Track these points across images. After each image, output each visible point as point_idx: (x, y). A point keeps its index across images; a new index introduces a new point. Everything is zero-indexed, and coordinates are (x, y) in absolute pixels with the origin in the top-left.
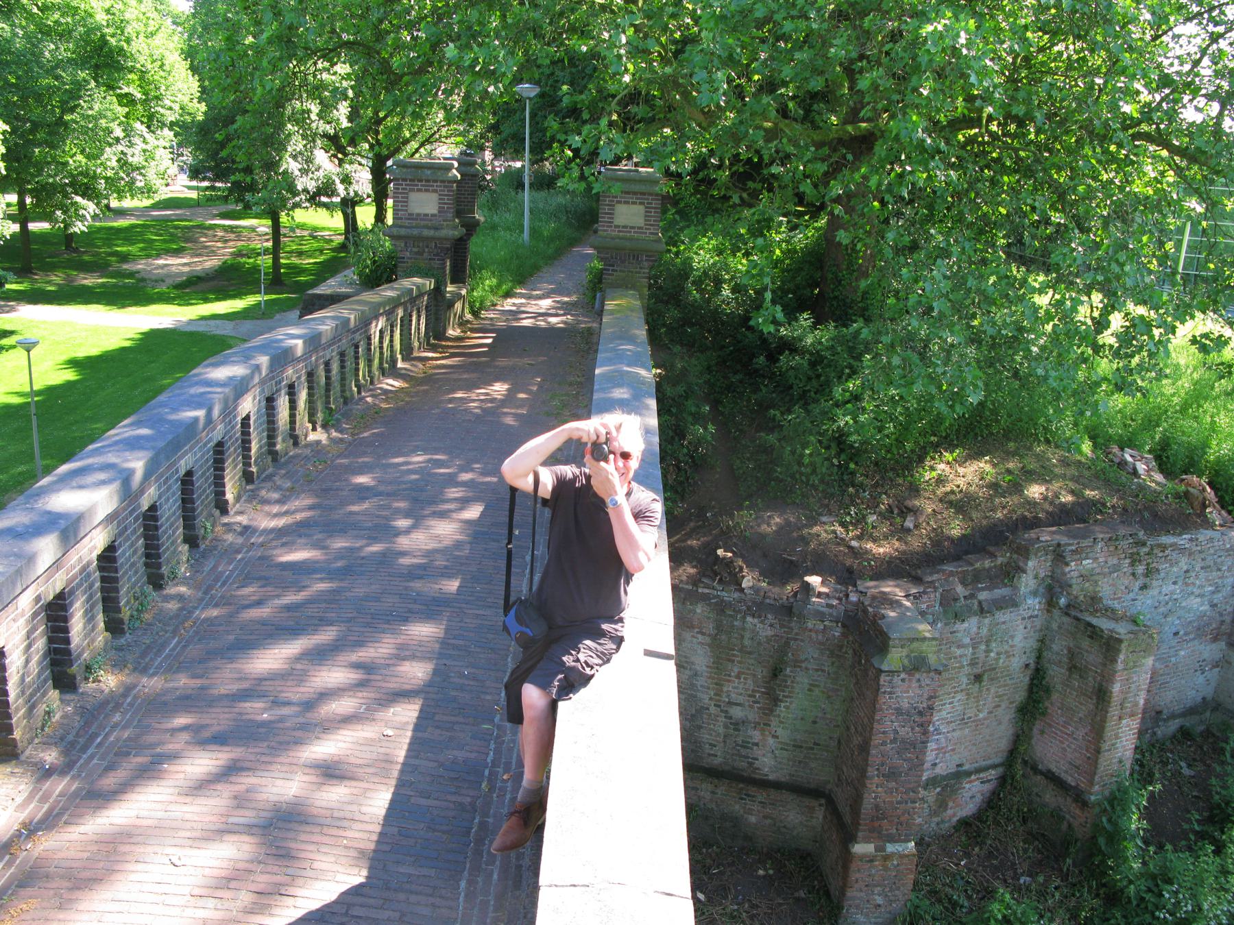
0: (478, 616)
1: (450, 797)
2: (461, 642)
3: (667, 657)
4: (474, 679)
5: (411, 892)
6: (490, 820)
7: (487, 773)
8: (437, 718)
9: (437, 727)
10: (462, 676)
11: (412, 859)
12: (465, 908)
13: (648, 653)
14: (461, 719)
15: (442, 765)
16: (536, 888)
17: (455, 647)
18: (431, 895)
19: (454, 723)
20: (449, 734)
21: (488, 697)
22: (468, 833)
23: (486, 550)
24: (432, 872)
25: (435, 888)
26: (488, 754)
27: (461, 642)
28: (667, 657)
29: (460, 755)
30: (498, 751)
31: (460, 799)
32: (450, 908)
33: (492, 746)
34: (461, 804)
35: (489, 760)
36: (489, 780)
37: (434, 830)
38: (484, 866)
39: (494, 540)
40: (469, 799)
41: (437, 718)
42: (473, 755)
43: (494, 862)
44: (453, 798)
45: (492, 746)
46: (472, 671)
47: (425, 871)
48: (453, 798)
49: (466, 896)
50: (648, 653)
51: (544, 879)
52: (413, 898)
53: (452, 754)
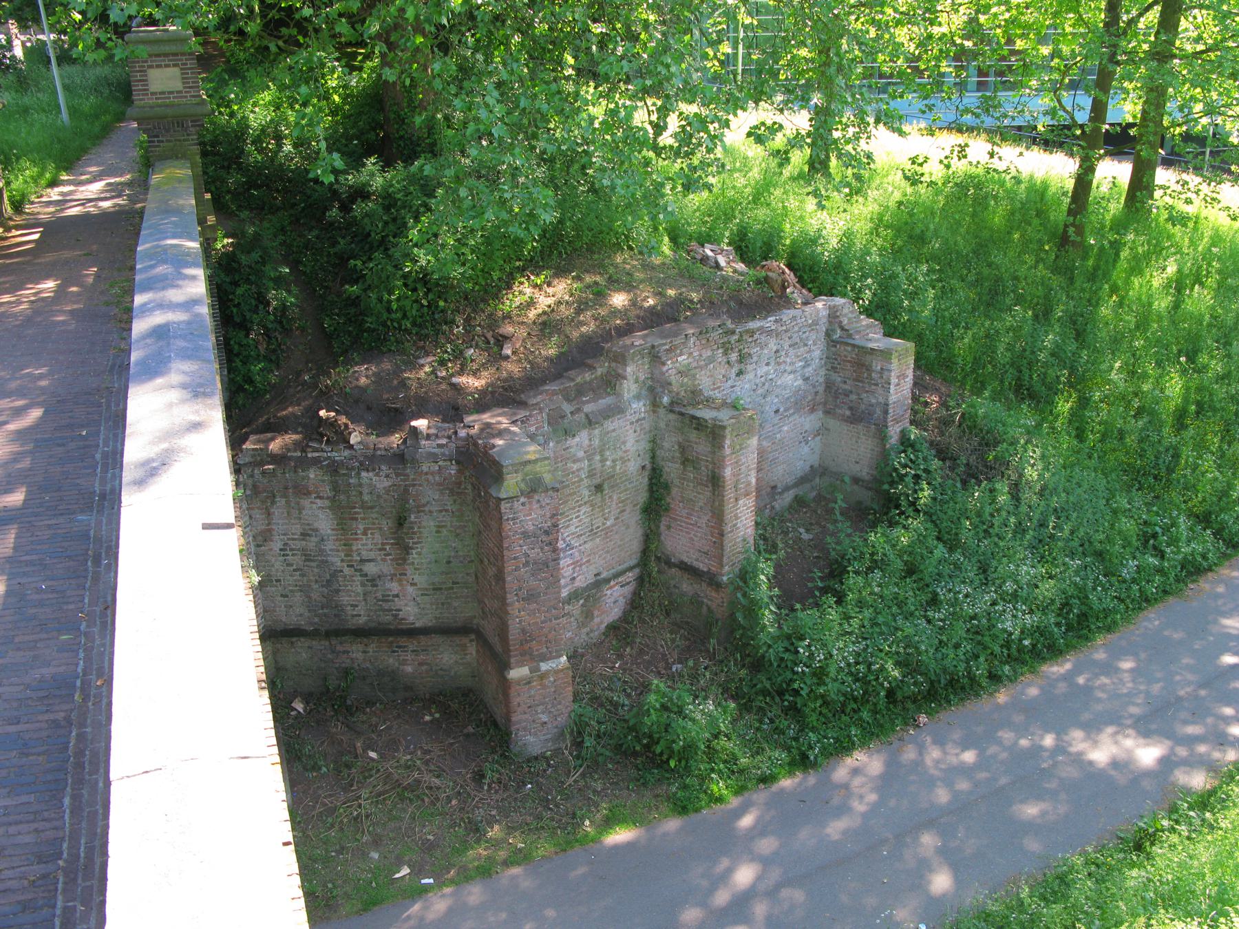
0: (49, 526)
1: (40, 718)
2: (34, 557)
3: (229, 526)
4: (53, 591)
5: (10, 824)
6: (89, 730)
7: (78, 683)
8: (17, 640)
9: (19, 649)
10: (39, 591)
11: (7, 790)
12: (71, 825)
13: (207, 526)
14: (45, 636)
15: (28, 686)
16: (108, 784)
17: (28, 563)
18: (33, 821)
19: (36, 642)
20: (32, 653)
21: (71, 607)
22: (67, 748)
23: (51, 457)
24: (32, 798)
25: (35, 813)
26: (77, 665)
27: (34, 557)
28: (229, 526)
29: (47, 672)
30: (88, 659)
31: (52, 716)
32: (56, 828)
33: (82, 655)
34: (54, 721)
35: (80, 670)
36: (83, 689)
37: (27, 755)
38: (87, 777)
39: (59, 445)
40: (62, 714)
41: (17, 640)
42: (62, 669)
43: (98, 770)
44: (46, 717)
45: (82, 655)
46: (50, 583)
47: (24, 799)
48: (46, 717)
49: (71, 812)
50: (207, 526)
51: (113, 775)
52: (12, 830)
53: (37, 674)
